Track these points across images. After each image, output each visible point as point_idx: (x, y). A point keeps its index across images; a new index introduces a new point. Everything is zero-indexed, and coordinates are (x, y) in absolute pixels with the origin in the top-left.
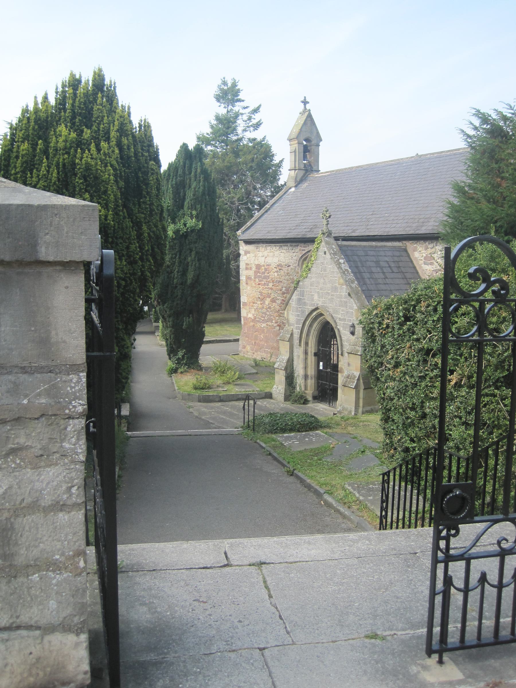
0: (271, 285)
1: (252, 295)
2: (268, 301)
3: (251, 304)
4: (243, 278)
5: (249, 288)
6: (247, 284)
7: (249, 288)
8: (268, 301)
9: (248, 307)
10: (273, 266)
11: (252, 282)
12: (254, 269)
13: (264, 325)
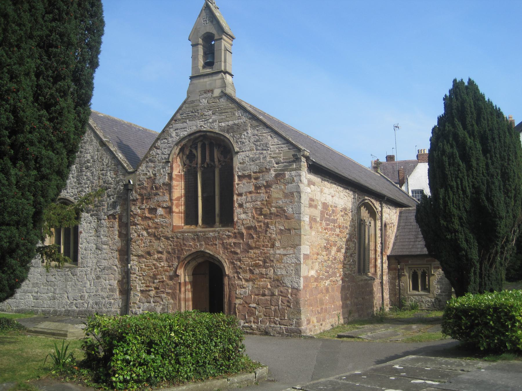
0: (338, 230)
1: (317, 243)
2: (334, 250)
3: (316, 256)
4: (306, 219)
5: (313, 233)
6: (311, 228)
7: (313, 233)
8: (334, 250)
9: (310, 262)
10: (340, 207)
11: (318, 225)
12: (320, 207)
13: (328, 282)
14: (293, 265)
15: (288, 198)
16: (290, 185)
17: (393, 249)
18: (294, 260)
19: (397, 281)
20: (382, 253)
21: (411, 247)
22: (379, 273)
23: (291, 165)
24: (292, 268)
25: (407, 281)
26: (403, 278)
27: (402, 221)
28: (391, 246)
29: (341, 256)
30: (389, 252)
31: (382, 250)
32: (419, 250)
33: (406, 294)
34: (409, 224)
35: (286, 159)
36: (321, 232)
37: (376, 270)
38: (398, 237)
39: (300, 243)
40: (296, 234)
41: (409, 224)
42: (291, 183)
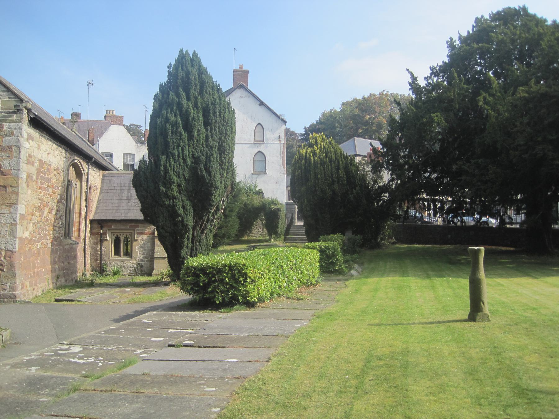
0: (50, 190)
3: (30, 216)
4: (24, 176)
5: (30, 192)
6: (28, 186)
9: (25, 222)
10: (54, 166)
12: (36, 165)
13: (39, 245)
14: (8, 225)
15: (5, 152)
16: (8, 138)
17: (96, 213)
18: (9, 220)
19: (99, 246)
20: (86, 217)
21: (114, 211)
22: (82, 237)
23: (10, 116)
24: (6, 229)
25: (109, 245)
26: (105, 243)
27: (105, 185)
28: (94, 209)
29: (52, 217)
30: (91, 216)
31: (86, 213)
32: (123, 215)
33: (107, 259)
34: (113, 188)
35: (6, 109)
36: (36, 191)
37: (79, 234)
38: (101, 201)
39: (17, 202)
40: (13, 192)
41: (113, 188)
42: (10, 136)
